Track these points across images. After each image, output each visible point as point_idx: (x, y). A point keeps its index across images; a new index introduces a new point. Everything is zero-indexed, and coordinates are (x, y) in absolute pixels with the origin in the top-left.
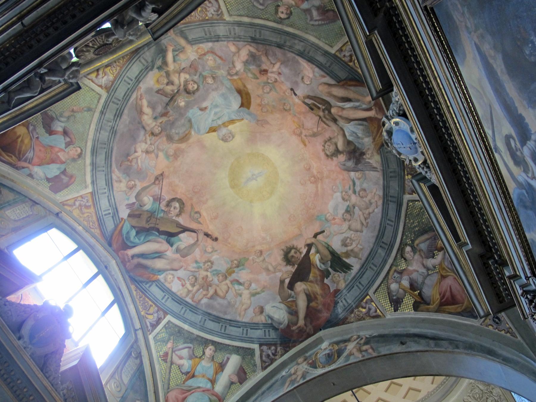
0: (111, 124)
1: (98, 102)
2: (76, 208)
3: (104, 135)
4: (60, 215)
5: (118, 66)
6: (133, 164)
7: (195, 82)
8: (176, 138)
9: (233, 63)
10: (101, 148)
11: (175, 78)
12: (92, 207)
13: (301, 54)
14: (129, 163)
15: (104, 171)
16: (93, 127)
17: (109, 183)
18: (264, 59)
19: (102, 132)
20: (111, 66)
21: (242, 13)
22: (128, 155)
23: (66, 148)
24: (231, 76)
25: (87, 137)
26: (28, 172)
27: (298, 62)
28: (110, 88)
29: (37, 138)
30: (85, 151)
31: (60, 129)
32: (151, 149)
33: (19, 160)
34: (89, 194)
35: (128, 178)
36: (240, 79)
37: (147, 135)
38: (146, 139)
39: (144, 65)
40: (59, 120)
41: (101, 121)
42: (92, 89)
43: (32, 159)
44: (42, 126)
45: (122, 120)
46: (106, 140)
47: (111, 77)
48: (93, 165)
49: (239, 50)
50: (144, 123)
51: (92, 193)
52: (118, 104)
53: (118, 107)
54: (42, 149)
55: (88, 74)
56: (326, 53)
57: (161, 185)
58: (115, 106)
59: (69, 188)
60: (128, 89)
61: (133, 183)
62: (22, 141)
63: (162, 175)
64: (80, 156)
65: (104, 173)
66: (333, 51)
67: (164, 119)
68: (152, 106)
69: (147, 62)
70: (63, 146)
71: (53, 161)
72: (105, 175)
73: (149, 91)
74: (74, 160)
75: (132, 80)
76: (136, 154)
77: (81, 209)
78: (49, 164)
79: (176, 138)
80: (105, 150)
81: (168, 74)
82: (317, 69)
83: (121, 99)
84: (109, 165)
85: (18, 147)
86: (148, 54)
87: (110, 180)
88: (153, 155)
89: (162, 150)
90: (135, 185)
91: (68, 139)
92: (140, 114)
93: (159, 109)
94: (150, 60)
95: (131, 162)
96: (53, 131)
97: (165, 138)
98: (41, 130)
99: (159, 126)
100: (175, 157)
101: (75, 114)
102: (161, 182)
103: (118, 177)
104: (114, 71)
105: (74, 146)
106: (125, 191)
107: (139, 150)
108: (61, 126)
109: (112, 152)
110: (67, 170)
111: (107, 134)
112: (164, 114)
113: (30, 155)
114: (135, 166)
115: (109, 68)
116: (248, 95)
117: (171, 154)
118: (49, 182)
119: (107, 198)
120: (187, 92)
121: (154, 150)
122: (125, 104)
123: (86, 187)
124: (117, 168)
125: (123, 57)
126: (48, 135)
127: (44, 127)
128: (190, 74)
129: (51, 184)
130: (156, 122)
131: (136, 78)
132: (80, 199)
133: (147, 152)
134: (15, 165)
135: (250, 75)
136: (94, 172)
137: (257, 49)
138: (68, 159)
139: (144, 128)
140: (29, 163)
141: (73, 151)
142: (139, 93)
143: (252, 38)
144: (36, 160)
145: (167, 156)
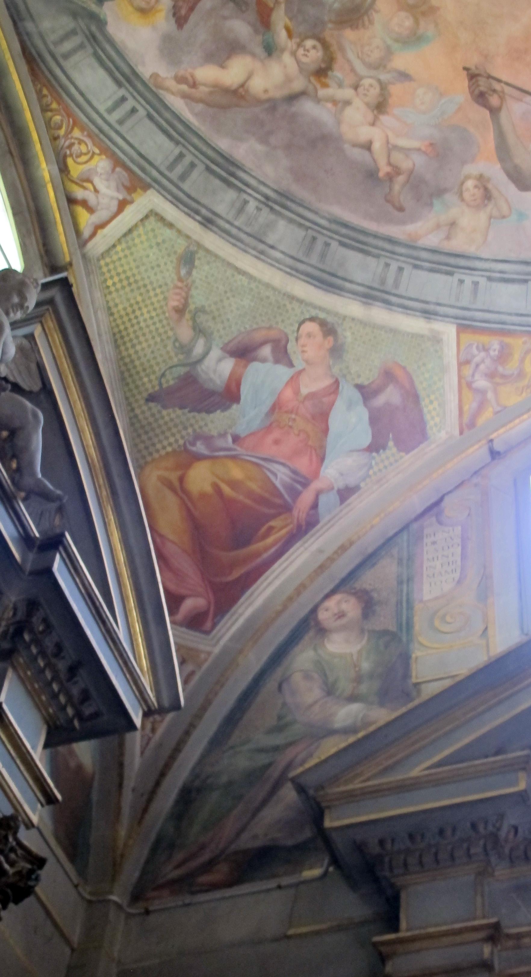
0: (252, 205)
1: (171, 225)
2: (496, 392)
3: (284, 234)
4: (497, 446)
5: (69, 132)
6: (405, 164)
10: (323, 256)
12: (508, 340)
14: (401, 179)
15: (401, 269)
16: (246, 262)
17: (447, 262)
19: (271, 239)
20: (65, 157)
22: (371, 174)
23: (291, 365)
25: (274, 289)
26: (333, 497)
28: (136, 178)
29: (236, 439)
30: (321, 309)
31: (227, 366)
32: (375, 91)
33: (287, 508)
34: (463, 336)
35: (448, 197)
37: (322, 92)
38: (335, 102)
39: (82, 46)
40: (200, 361)
41: (234, 231)
42: (125, 235)
43: (295, 472)
44: (204, 415)
45: (248, 163)
46: (301, 233)
47: (102, 164)
48: (370, 295)
50: (278, 94)
51: (462, 329)
52: (192, 165)
53: (201, 167)
54: (276, 434)
55: (78, 233)
57: (507, 89)
58: (195, 174)
59: (422, 393)
60: (150, 117)
61: (470, 184)
62: (234, 484)
63: (473, 77)
64: (328, 329)
65: (408, 270)
68: (225, 49)
69: (73, 32)
70: (283, 373)
71: (322, 418)
72: (416, 267)
73: (170, 49)
74: (336, 351)
75: (123, 99)
76: (377, 146)
77: (503, 376)
78: (326, 431)
80: (334, 245)
83: (177, 151)
84: (387, 246)
85: (248, 502)
86: (46, 25)
87: (436, 258)
88: (396, 90)
89: (389, 52)
91: (266, 351)
92: (242, 97)
93: (240, 28)
94: (66, 23)
95: (397, 171)
96: (228, 388)
97: (349, 34)
98: (216, 422)
99: (299, 45)
100: (424, 14)
101: (192, 307)
102: (497, 86)
103: (438, 226)
104: (84, 149)
105: (292, 338)
106: (490, 217)
107: (365, 133)
108: (220, 360)
109: (345, 225)
110: (363, 381)
111: (282, 224)
113: (281, 476)
114: (419, 160)
115: (70, 161)
117: (409, 23)
118: (384, 447)
119: (494, 285)
121: (379, 81)
122: (196, 141)
123: (436, 339)
124: (403, 223)
125: (45, 109)
126: (235, 406)
127: (209, 412)
129: (391, 444)
130: (283, 50)
131: (119, 84)
132: (468, 371)
133: (380, 107)
134: (299, 527)
136: (393, 299)
138: (330, 368)
139: (293, 98)
140: (305, 484)
141: (308, 346)
142: (171, 84)
144: (303, 464)
145: (413, 39)
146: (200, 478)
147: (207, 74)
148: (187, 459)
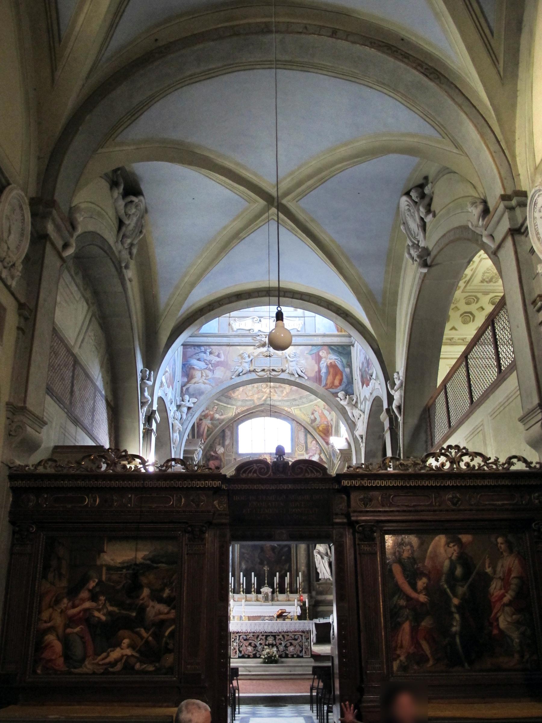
3: (304, 400)
11: (268, 391)
16: (305, 406)
31: (313, 416)
33: (329, 426)
49: (237, 396)
68: (282, 391)
70: (317, 413)
71: (324, 414)
73: (279, 396)
74: (319, 407)
93: (281, 389)
98: (317, 422)
113: (326, 423)
146: (321, 428)
147: (283, 395)
148: (318, 427)
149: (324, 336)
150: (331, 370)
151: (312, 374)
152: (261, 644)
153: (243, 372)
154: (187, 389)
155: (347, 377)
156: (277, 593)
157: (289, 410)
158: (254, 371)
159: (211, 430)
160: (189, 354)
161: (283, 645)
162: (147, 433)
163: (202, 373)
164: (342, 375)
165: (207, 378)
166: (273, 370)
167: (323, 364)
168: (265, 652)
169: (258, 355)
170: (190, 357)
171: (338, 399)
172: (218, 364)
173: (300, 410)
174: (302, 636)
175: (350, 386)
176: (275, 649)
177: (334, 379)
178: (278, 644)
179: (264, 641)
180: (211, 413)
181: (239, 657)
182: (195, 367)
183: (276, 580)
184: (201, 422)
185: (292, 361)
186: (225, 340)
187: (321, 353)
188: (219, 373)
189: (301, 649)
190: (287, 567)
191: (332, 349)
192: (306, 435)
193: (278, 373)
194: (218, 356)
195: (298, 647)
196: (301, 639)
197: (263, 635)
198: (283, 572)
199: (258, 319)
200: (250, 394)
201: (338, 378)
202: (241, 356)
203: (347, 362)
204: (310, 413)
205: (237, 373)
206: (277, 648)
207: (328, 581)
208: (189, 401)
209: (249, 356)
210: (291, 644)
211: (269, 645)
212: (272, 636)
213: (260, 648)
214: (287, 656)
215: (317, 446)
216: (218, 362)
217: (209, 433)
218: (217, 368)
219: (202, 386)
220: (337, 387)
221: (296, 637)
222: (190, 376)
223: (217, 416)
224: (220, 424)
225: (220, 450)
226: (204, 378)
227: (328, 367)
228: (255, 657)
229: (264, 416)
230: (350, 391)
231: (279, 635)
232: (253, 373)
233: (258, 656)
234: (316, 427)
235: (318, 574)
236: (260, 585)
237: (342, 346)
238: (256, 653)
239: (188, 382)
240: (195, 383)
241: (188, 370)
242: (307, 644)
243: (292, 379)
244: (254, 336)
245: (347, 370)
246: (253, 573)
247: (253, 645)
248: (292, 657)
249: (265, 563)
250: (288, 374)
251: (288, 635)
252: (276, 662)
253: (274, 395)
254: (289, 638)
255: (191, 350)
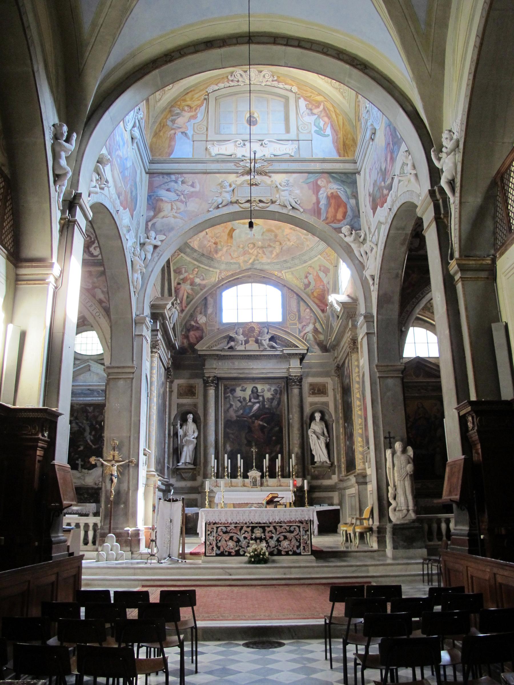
3: (297, 261)
7: (248, 247)
8: (273, 234)
9: (227, 251)
11: (255, 252)
13: (196, 251)
16: (297, 268)
17: (312, 249)
18: (212, 250)
21: (211, 273)
22: (296, 247)
24: (231, 246)
27: (199, 247)
31: (306, 280)
33: (325, 290)
36: (228, 243)
49: (221, 257)
56: (184, 253)
66: (182, 254)
67: (271, 244)
68: (271, 252)
70: (311, 275)
71: (319, 277)
74: (313, 268)
79: (273, 234)
81: (257, 256)
82: (191, 245)
88: (288, 236)
90: (304, 238)
93: (270, 249)
98: (311, 287)
112: (270, 246)
116: (229, 234)
120: (254, 245)
123: (319, 258)
128: (248, 251)
133: (289, 240)
135: (222, 243)
137: (213, 255)
141: (311, 271)
143: (213, 260)
144: (322, 284)
146: (315, 294)
147: (273, 256)
148: (313, 293)
149: (324, 161)
150: (333, 201)
151: (309, 207)
152: (245, 538)
153: (224, 204)
154: (153, 225)
155: (352, 210)
156: (267, 477)
157: (279, 275)
158: (237, 202)
159: (191, 297)
160: (156, 184)
161: (275, 538)
162: (67, 226)
163: (172, 205)
164: (346, 208)
165: (178, 211)
166: (261, 201)
167: (323, 195)
168: (250, 549)
169: (242, 183)
170: (157, 187)
171: (342, 235)
172: (191, 195)
173: (292, 274)
174: (299, 527)
175: (356, 220)
176: (264, 544)
177: (336, 211)
178: (268, 538)
179: (250, 534)
180: (191, 276)
181: (217, 555)
182: (163, 198)
183: (266, 462)
184: (179, 286)
185: (284, 191)
186: (200, 167)
187: (319, 182)
188: (193, 206)
189: (298, 544)
190: (278, 448)
191: (333, 178)
192: (298, 303)
193: (266, 205)
194: (193, 186)
195: (294, 542)
196: (298, 531)
197: (248, 527)
198: (273, 454)
199: (242, 142)
200: (235, 255)
201: (341, 210)
202: (221, 185)
203: (353, 192)
204: (303, 277)
205: (215, 204)
206: (267, 542)
207: (325, 464)
208: (155, 238)
209: (230, 186)
210: (285, 538)
211: (256, 539)
212: (260, 527)
213: (244, 543)
214: (279, 553)
215: (312, 315)
216: (192, 192)
217: (189, 299)
218: (190, 200)
219: (172, 220)
220: (340, 221)
221: (292, 529)
222: (157, 210)
223: (197, 281)
224: (201, 290)
225: (202, 320)
226: (174, 211)
227: (328, 198)
228: (237, 554)
229: (252, 282)
230: (356, 225)
231: (269, 527)
232: (235, 205)
233: (242, 553)
234: (310, 292)
235: (313, 456)
236: (247, 468)
237: (345, 174)
238: (240, 549)
239: (154, 216)
240: (163, 217)
241: (154, 202)
242: (305, 537)
243: (284, 211)
244: (237, 161)
245: (353, 201)
246: (239, 456)
247: (235, 539)
248: (287, 554)
249: (253, 444)
250: (278, 206)
251: (281, 527)
252: (265, 561)
253: (262, 257)
254: (282, 530)
255: (158, 180)
